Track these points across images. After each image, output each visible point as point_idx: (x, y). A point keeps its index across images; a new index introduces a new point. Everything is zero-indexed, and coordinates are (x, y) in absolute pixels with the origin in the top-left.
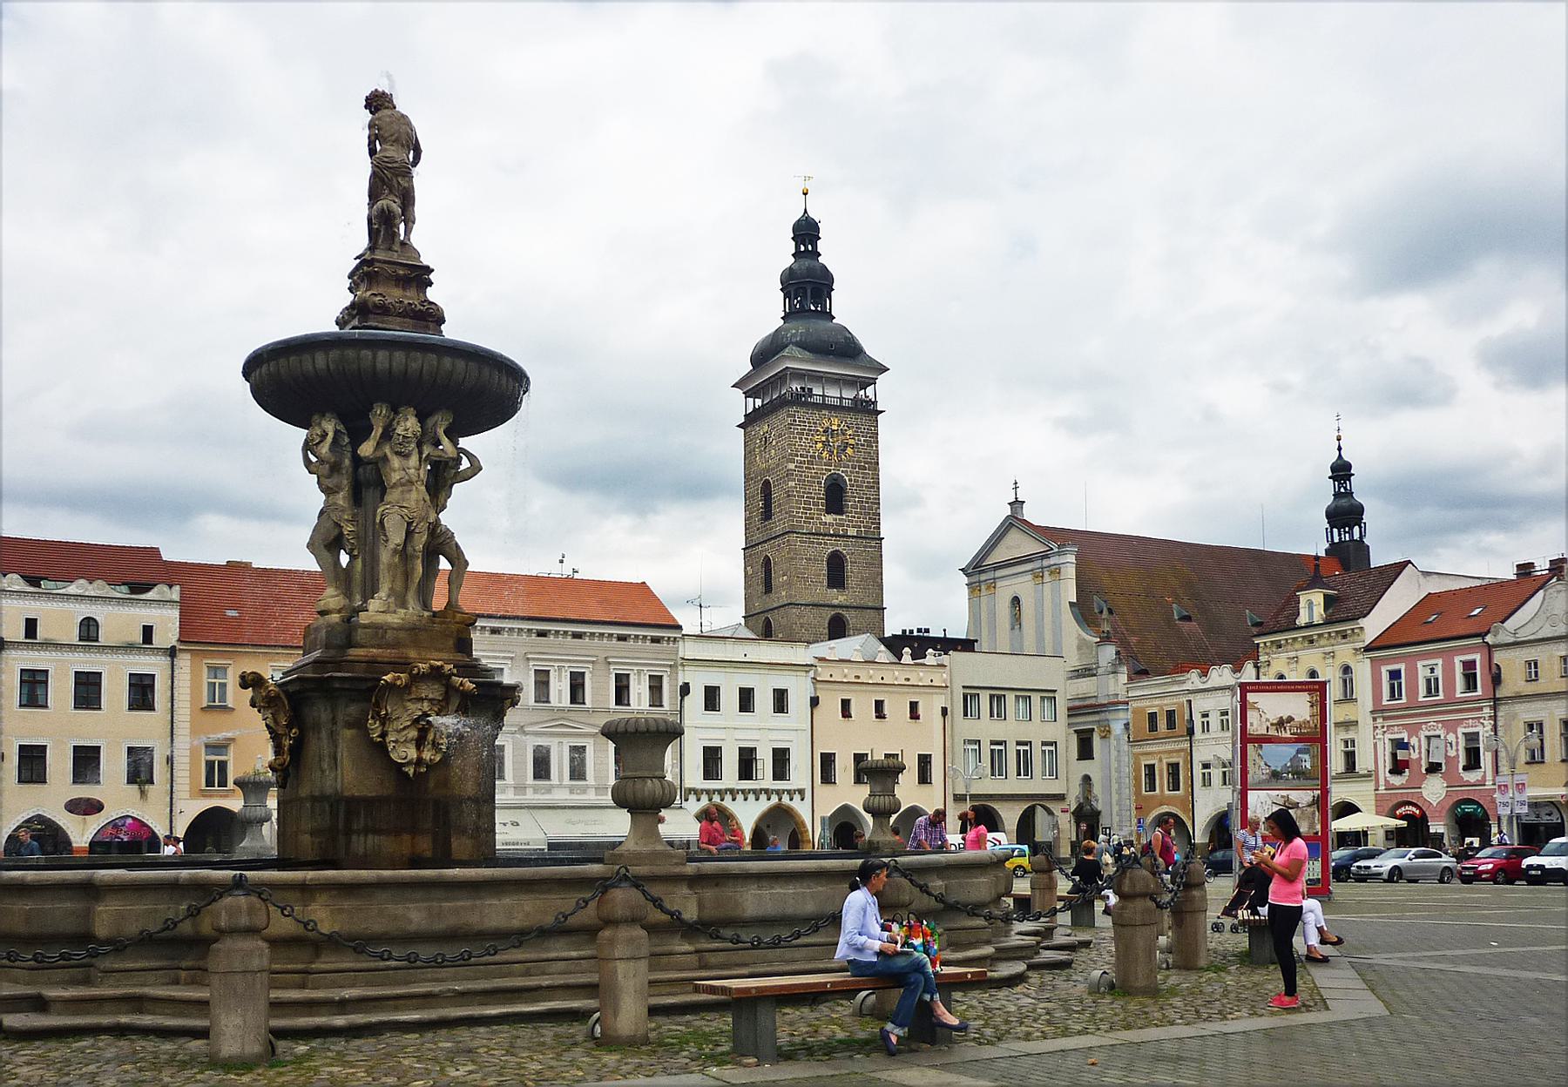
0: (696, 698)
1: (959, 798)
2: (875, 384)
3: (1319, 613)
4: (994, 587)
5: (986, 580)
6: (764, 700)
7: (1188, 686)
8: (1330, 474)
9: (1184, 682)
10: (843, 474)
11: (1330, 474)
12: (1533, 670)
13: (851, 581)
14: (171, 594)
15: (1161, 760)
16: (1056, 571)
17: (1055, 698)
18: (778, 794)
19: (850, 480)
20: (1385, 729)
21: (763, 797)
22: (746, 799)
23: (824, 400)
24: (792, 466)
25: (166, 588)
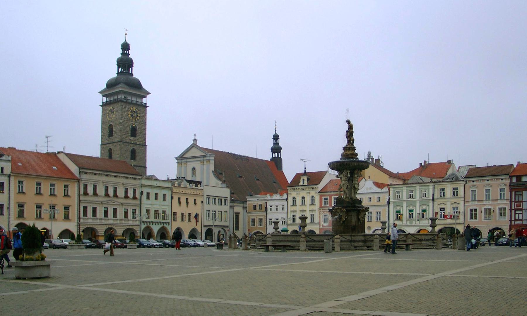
0: (145, 195)
1: (205, 226)
2: (146, 98)
3: (306, 183)
4: (187, 164)
5: (184, 162)
6: (160, 197)
7: (266, 198)
8: (273, 138)
9: (265, 197)
10: (136, 125)
11: (273, 138)
12: (370, 200)
13: (137, 158)
14: (9, 158)
15: (257, 218)
16: (208, 161)
17: (227, 200)
18: (163, 224)
19: (138, 127)
20: (323, 212)
21: (160, 224)
22: (155, 224)
23: (131, 101)
24: (121, 121)
25: (7, 156)
